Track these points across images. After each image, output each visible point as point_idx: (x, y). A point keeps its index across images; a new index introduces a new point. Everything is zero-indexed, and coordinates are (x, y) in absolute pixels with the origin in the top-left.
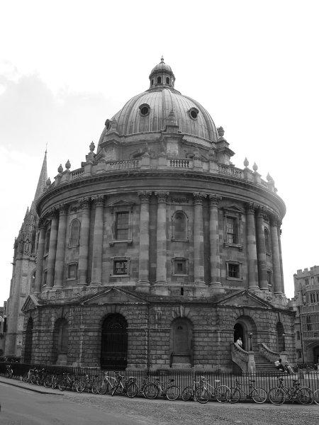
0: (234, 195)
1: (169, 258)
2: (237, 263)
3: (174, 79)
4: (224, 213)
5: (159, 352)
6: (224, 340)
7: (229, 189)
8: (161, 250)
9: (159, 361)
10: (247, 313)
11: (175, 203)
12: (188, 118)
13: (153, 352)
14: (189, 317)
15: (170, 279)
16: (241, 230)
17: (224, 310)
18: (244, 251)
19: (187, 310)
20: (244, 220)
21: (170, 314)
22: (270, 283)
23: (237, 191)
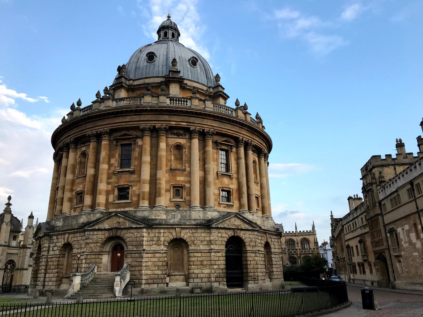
0: (124, 124)
1: (74, 193)
2: (126, 186)
3: (176, 30)
4: (117, 143)
5: (51, 275)
6: (88, 261)
7: (121, 119)
8: (68, 187)
9: (50, 283)
10: (119, 233)
11: (82, 145)
12: (145, 63)
13: (47, 275)
14: (71, 243)
15: (72, 211)
16: (135, 154)
17: (92, 233)
18: (137, 172)
19: (71, 236)
20: (140, 142)
21: (61, 242)
22: (182, 199)
23: (128, 119)
